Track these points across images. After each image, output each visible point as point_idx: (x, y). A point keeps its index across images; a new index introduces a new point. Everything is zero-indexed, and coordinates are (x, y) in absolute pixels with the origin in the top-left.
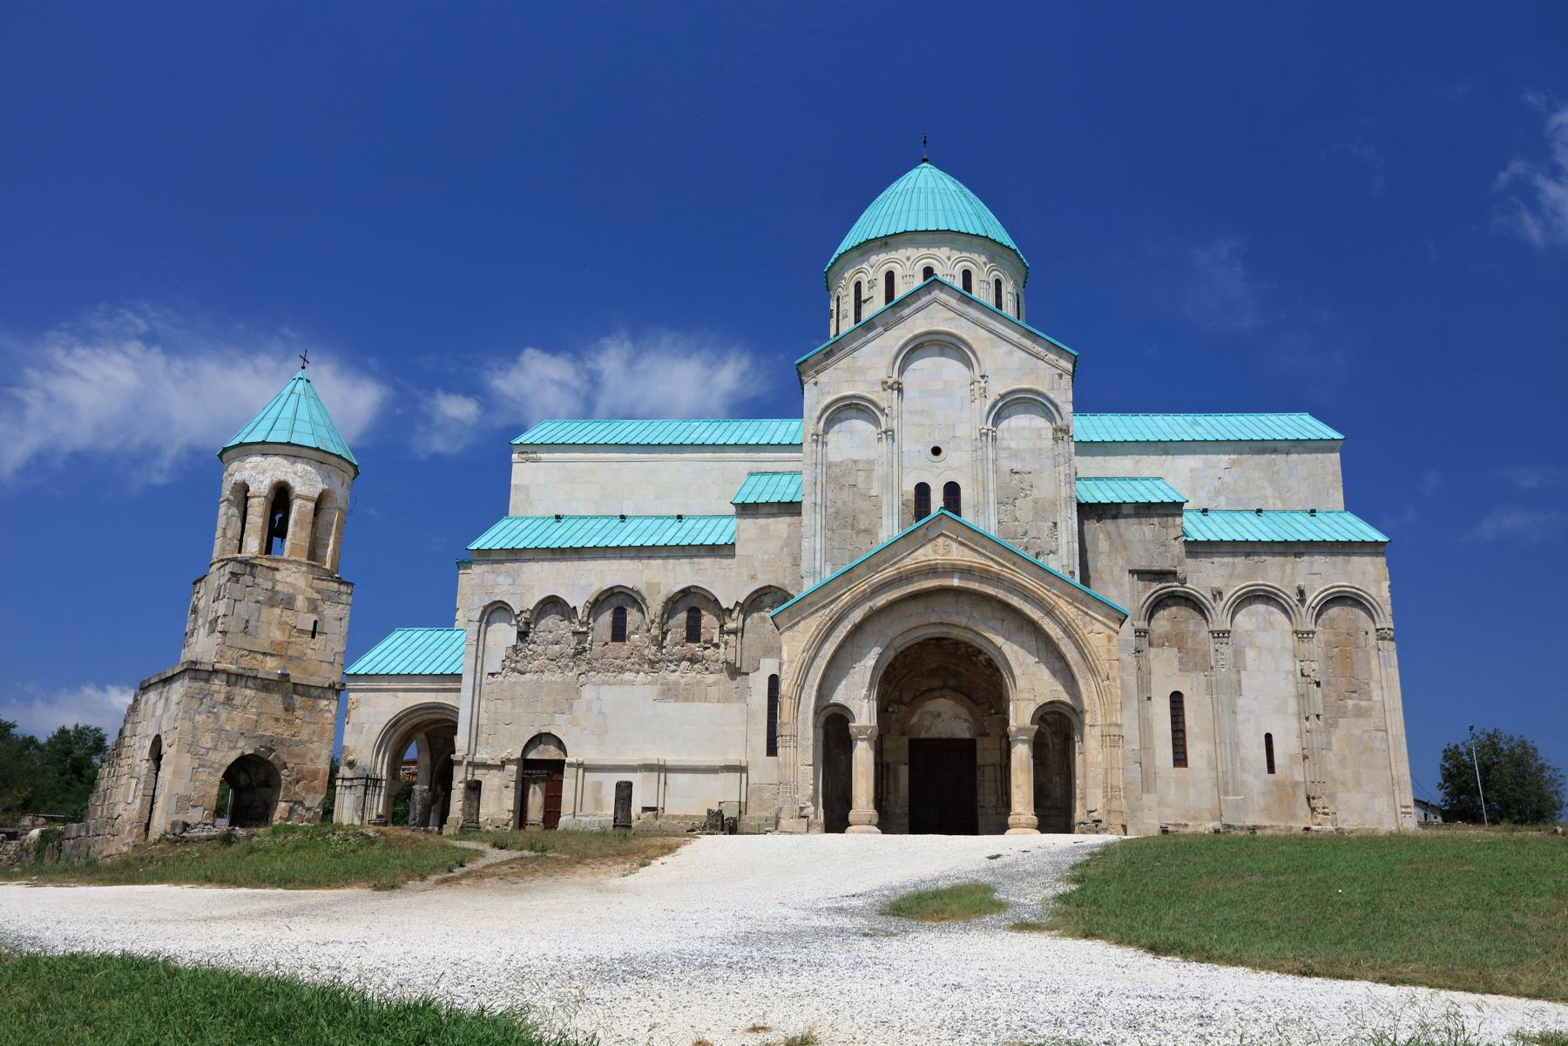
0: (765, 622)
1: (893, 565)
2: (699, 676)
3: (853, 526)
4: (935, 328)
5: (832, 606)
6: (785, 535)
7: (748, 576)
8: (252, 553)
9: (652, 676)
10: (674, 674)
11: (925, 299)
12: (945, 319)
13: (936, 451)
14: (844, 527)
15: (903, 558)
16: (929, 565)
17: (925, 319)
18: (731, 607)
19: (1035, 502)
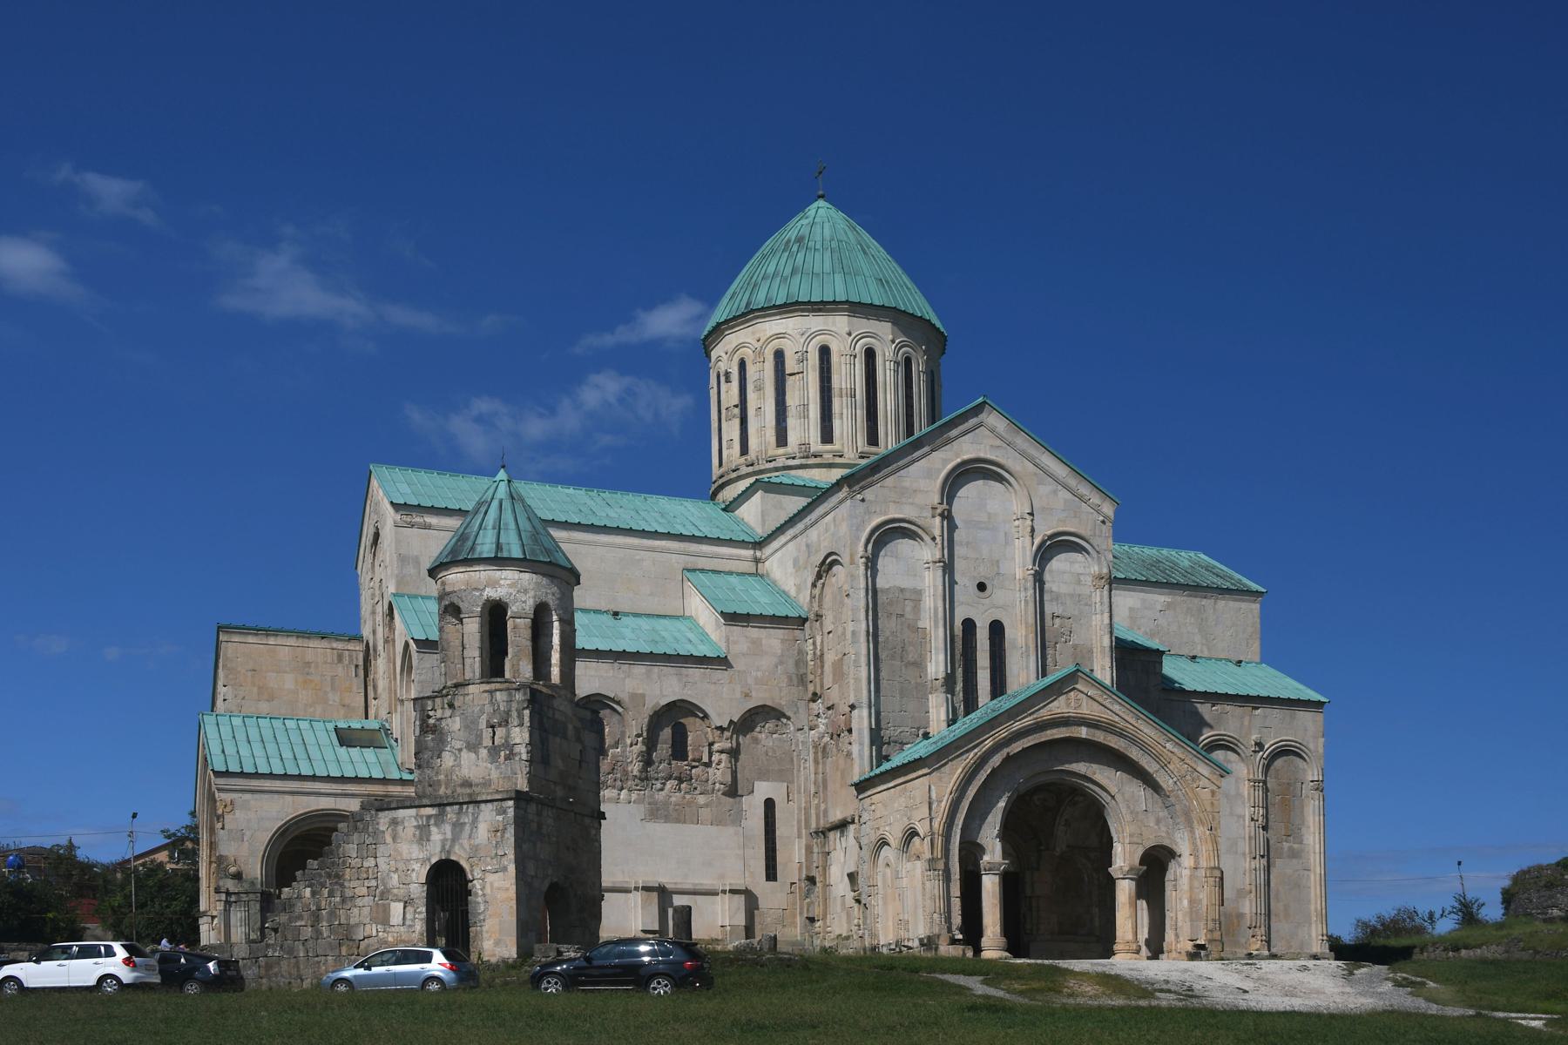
0: (757, 744)
1: (1030, 715)
2: (688, 797)
3: (901, 658)
4: (982, 455)
5: (976, 750)
6: (780, 651)
7: (742, 692)
8: (527, 678)
9: (638, 795)
10: (660, 793)
11: (972, 422)
12: (992, 446)
13: (982, 587)
14: (893, 657)
15: (1039, 709)
16: (1063, 717)
17: (972, 443)
18: (725, 725)
19: (1075, 647)
